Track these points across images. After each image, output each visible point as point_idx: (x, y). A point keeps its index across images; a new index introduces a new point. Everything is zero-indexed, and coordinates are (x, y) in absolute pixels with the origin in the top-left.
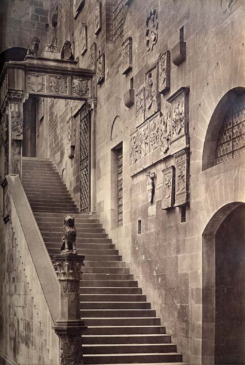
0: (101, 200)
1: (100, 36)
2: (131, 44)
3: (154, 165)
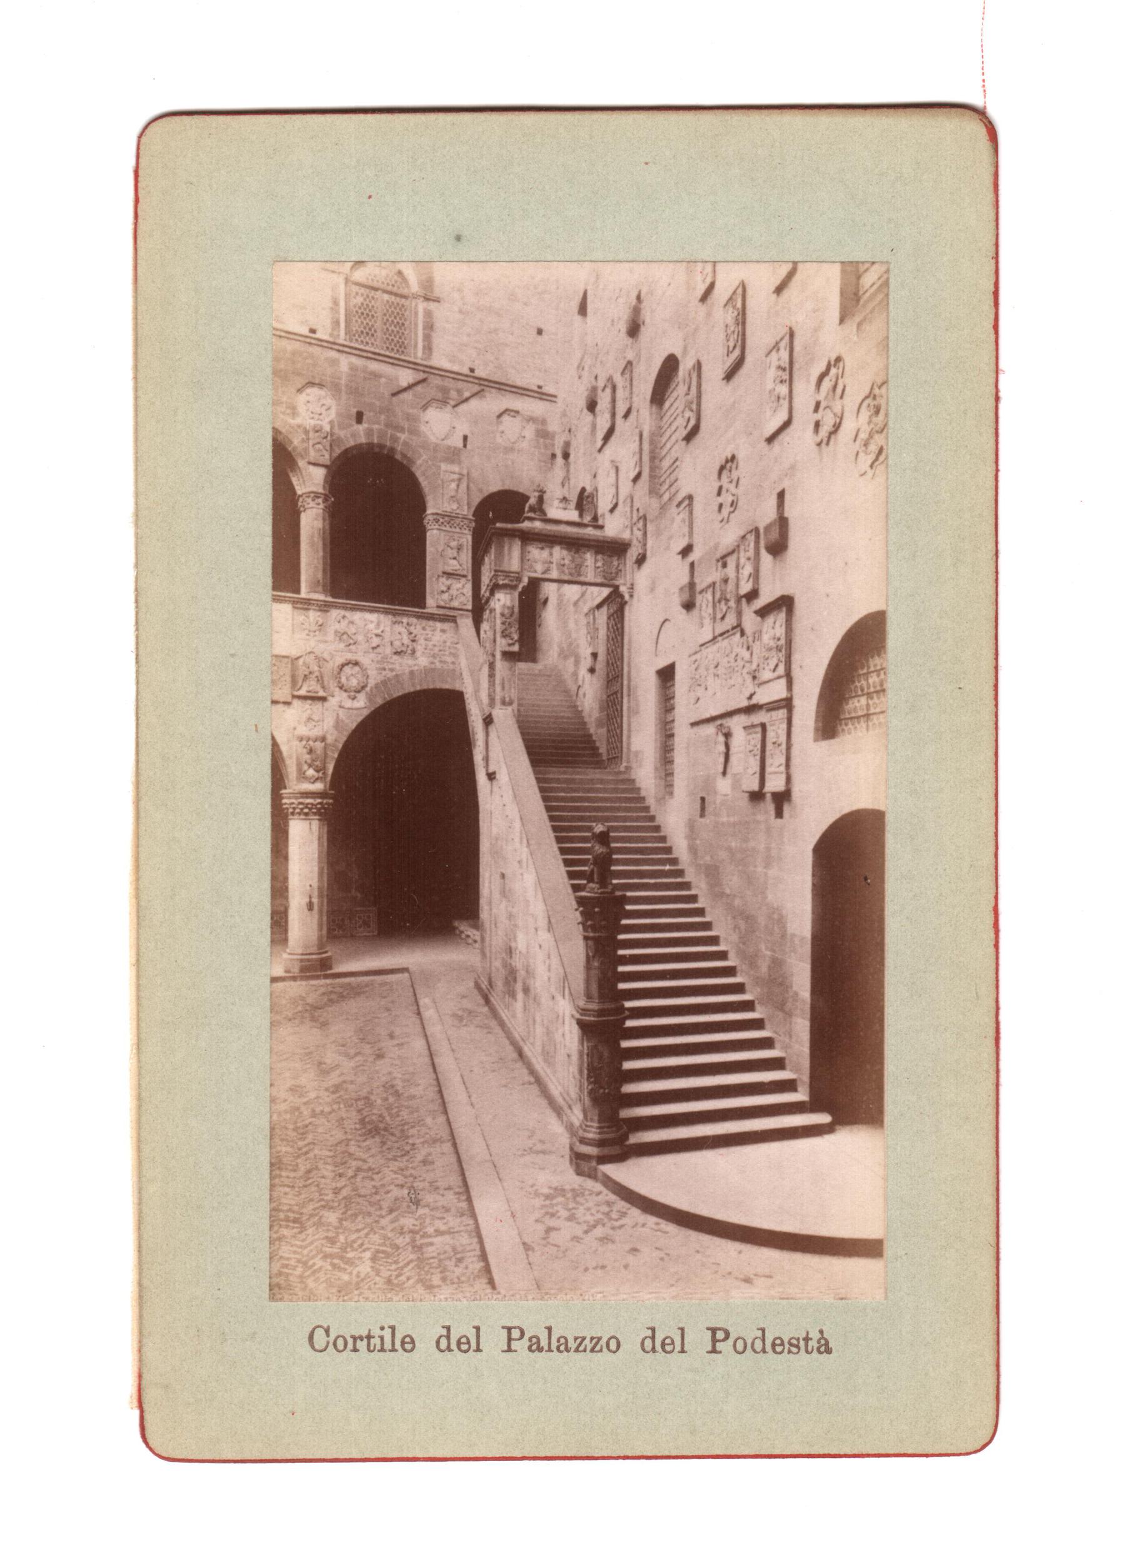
1: (641, 482)
2: (690, 505)
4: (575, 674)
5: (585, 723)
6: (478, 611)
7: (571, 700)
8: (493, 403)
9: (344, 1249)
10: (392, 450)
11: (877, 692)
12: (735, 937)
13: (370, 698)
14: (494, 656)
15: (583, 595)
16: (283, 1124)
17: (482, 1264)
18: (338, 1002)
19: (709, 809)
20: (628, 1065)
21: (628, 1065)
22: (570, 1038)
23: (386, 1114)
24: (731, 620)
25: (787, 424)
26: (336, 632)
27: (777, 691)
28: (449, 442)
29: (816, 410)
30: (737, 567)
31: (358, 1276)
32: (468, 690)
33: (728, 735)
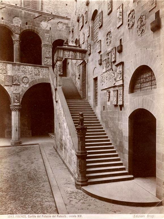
0: (90, 96)
1: (89, 38)
2: (101, 42)
3: (110, 88)
4: (75, 79)
5: (77, 90)
6: (53, 66)
7: (74, 84)
8: (56, 20)
9: (25, 205)
10: (34, 31)
11: (143, 83)
12: (111, 137)
13: (29, 85)
14: (57, 75)
15: (77, 62)
16: (11, 178)
17: (56, 208)
18: (23, 151)
19: (105, 108)
20: (88, 165)
21: (88, 165)
22: (75, 158)
23: (34, 176)
24: (110, 67)
25: (122, 24)
26: (22, 70)
27: (121, 83)
28: (47, 29)
29: (128, 21)
30: (111, 55)
31: (28, 211)
32: (51, 83)
33: (109, 92)
